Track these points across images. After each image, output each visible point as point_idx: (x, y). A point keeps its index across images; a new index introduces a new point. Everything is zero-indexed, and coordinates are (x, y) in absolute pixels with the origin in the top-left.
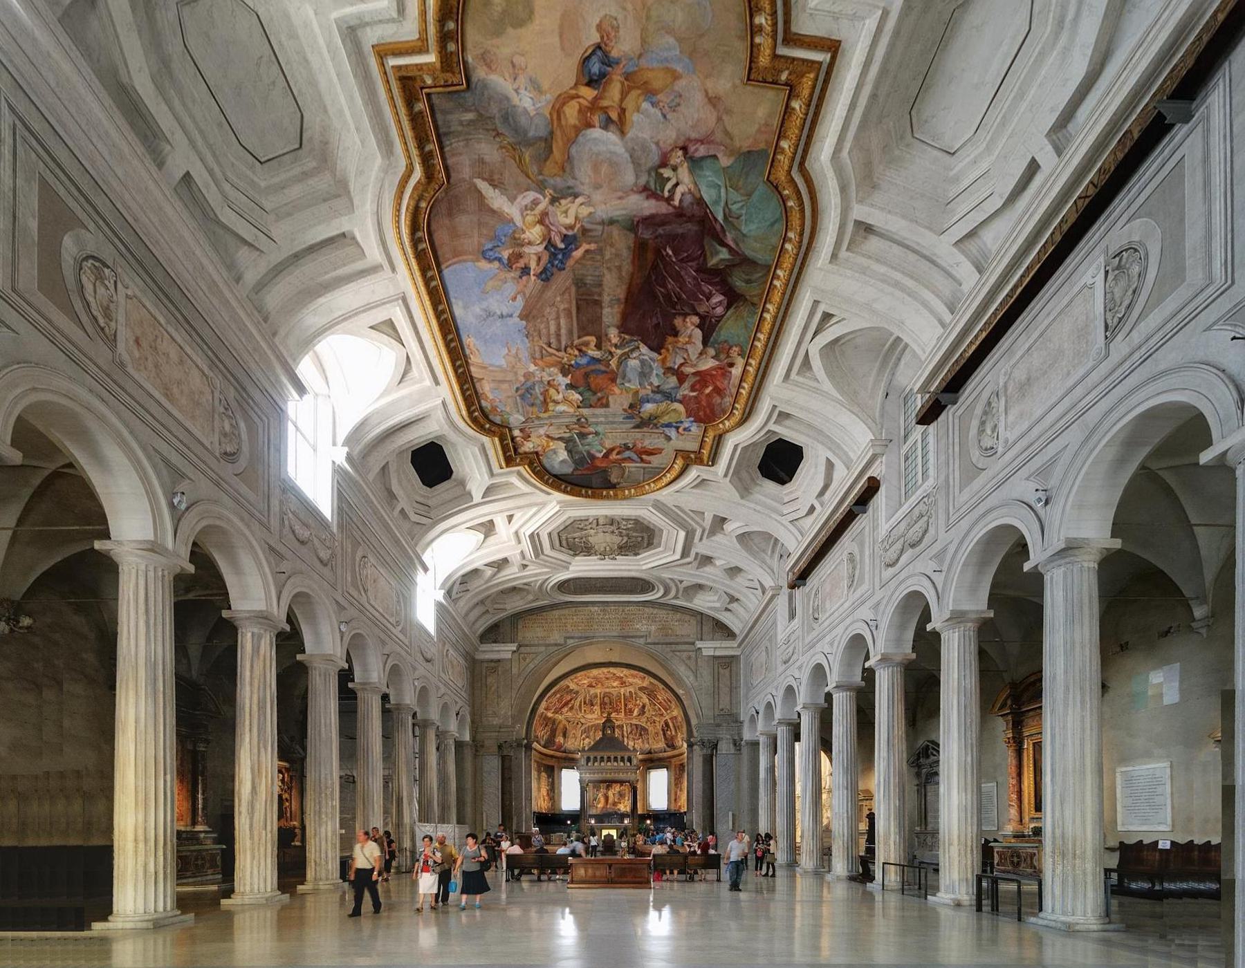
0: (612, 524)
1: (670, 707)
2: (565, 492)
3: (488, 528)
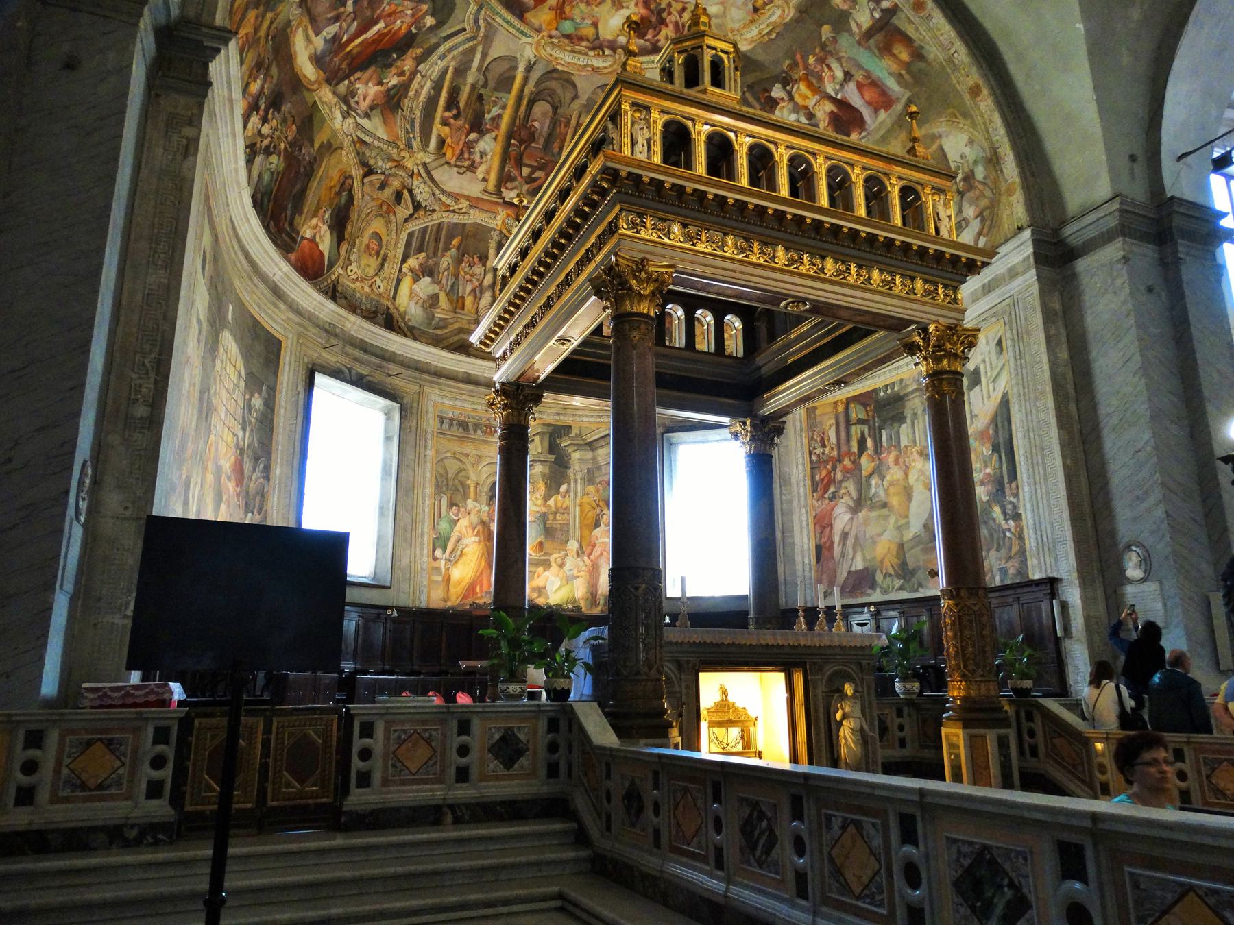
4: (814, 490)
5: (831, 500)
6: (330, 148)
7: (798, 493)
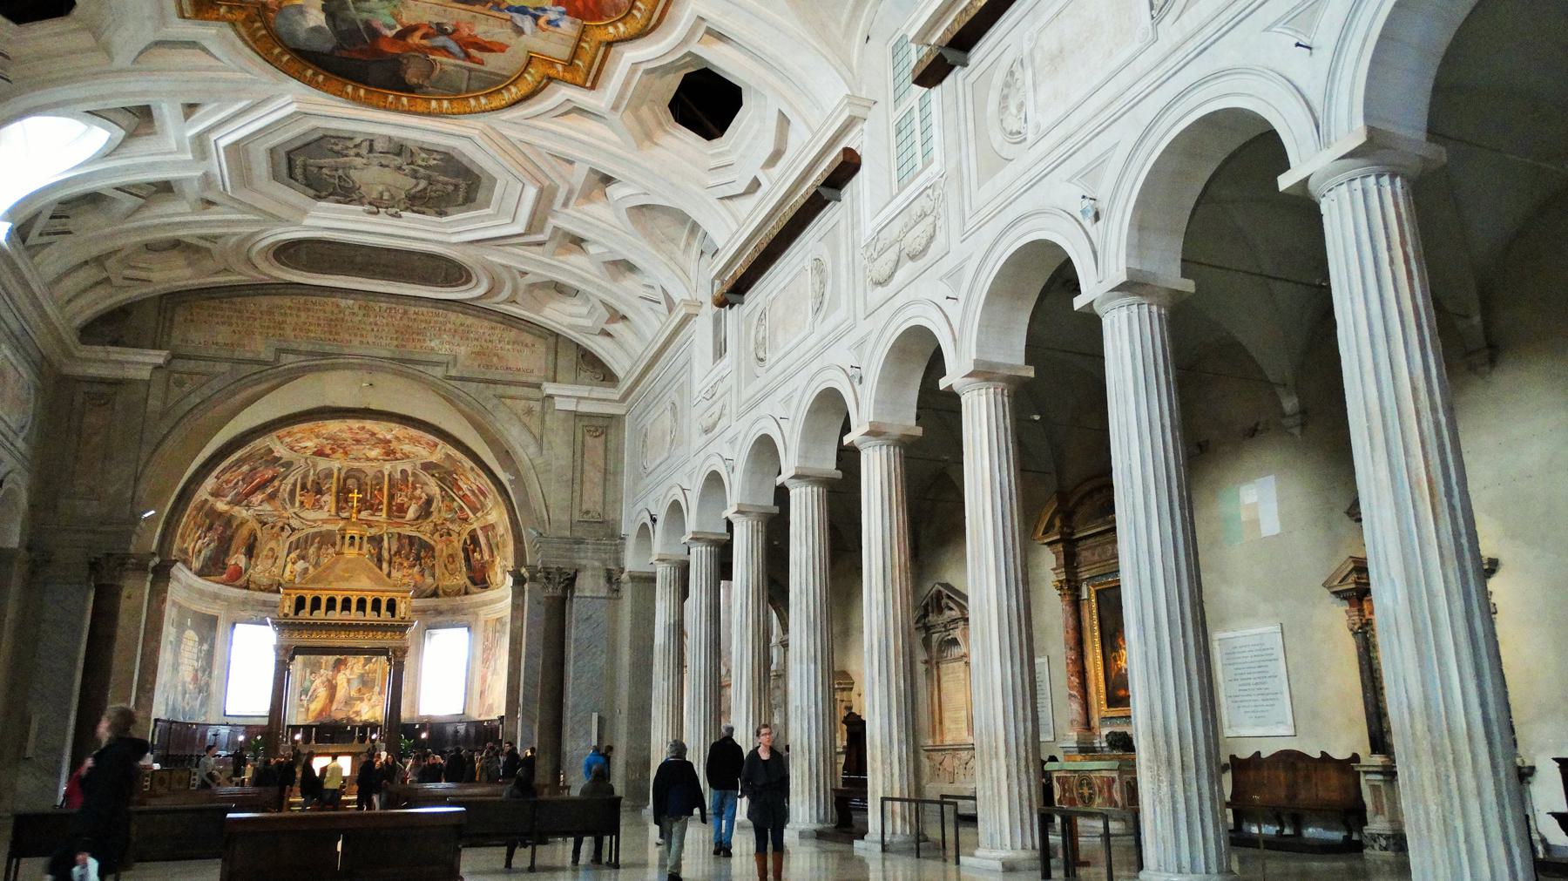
0: (399, 154)
1: (483, 505)
2: (311, 83)
3: (141, 119)
6: (242, 524)
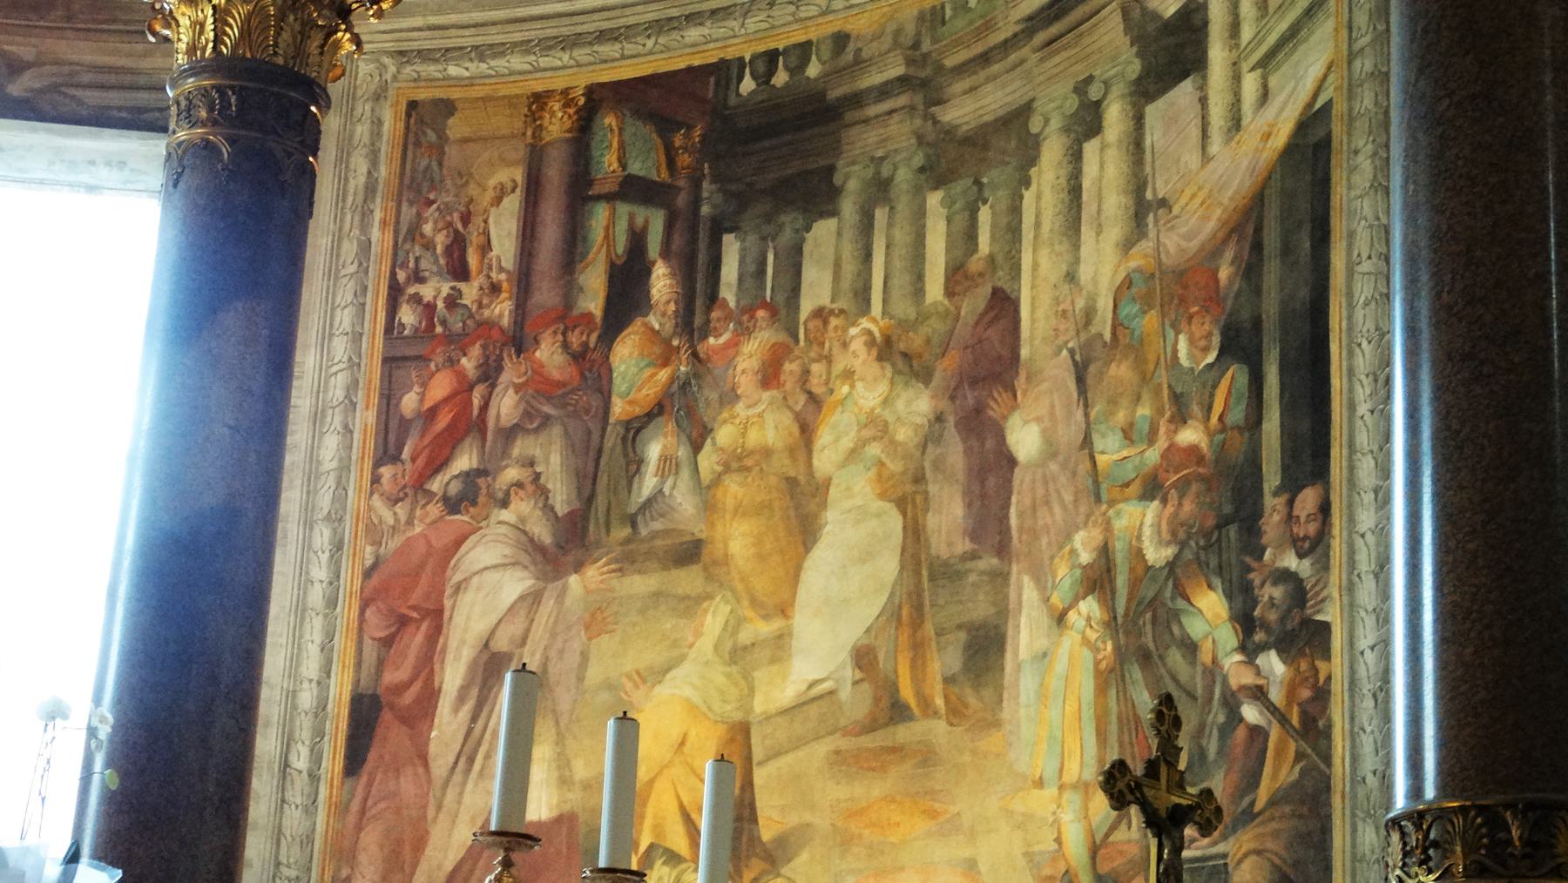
4: (387, 453)
5: (453, 505)
7: (313, 458)
